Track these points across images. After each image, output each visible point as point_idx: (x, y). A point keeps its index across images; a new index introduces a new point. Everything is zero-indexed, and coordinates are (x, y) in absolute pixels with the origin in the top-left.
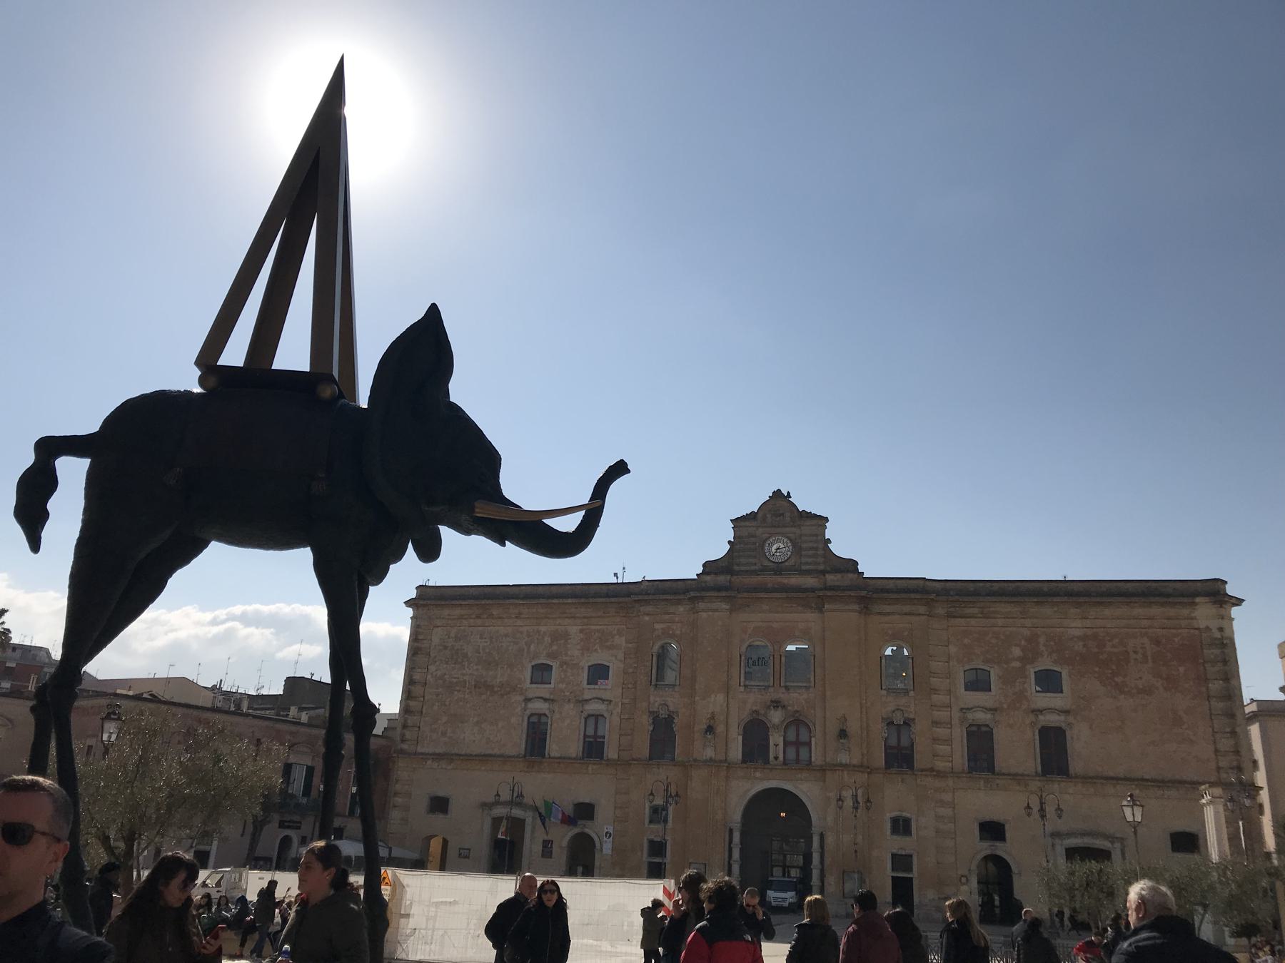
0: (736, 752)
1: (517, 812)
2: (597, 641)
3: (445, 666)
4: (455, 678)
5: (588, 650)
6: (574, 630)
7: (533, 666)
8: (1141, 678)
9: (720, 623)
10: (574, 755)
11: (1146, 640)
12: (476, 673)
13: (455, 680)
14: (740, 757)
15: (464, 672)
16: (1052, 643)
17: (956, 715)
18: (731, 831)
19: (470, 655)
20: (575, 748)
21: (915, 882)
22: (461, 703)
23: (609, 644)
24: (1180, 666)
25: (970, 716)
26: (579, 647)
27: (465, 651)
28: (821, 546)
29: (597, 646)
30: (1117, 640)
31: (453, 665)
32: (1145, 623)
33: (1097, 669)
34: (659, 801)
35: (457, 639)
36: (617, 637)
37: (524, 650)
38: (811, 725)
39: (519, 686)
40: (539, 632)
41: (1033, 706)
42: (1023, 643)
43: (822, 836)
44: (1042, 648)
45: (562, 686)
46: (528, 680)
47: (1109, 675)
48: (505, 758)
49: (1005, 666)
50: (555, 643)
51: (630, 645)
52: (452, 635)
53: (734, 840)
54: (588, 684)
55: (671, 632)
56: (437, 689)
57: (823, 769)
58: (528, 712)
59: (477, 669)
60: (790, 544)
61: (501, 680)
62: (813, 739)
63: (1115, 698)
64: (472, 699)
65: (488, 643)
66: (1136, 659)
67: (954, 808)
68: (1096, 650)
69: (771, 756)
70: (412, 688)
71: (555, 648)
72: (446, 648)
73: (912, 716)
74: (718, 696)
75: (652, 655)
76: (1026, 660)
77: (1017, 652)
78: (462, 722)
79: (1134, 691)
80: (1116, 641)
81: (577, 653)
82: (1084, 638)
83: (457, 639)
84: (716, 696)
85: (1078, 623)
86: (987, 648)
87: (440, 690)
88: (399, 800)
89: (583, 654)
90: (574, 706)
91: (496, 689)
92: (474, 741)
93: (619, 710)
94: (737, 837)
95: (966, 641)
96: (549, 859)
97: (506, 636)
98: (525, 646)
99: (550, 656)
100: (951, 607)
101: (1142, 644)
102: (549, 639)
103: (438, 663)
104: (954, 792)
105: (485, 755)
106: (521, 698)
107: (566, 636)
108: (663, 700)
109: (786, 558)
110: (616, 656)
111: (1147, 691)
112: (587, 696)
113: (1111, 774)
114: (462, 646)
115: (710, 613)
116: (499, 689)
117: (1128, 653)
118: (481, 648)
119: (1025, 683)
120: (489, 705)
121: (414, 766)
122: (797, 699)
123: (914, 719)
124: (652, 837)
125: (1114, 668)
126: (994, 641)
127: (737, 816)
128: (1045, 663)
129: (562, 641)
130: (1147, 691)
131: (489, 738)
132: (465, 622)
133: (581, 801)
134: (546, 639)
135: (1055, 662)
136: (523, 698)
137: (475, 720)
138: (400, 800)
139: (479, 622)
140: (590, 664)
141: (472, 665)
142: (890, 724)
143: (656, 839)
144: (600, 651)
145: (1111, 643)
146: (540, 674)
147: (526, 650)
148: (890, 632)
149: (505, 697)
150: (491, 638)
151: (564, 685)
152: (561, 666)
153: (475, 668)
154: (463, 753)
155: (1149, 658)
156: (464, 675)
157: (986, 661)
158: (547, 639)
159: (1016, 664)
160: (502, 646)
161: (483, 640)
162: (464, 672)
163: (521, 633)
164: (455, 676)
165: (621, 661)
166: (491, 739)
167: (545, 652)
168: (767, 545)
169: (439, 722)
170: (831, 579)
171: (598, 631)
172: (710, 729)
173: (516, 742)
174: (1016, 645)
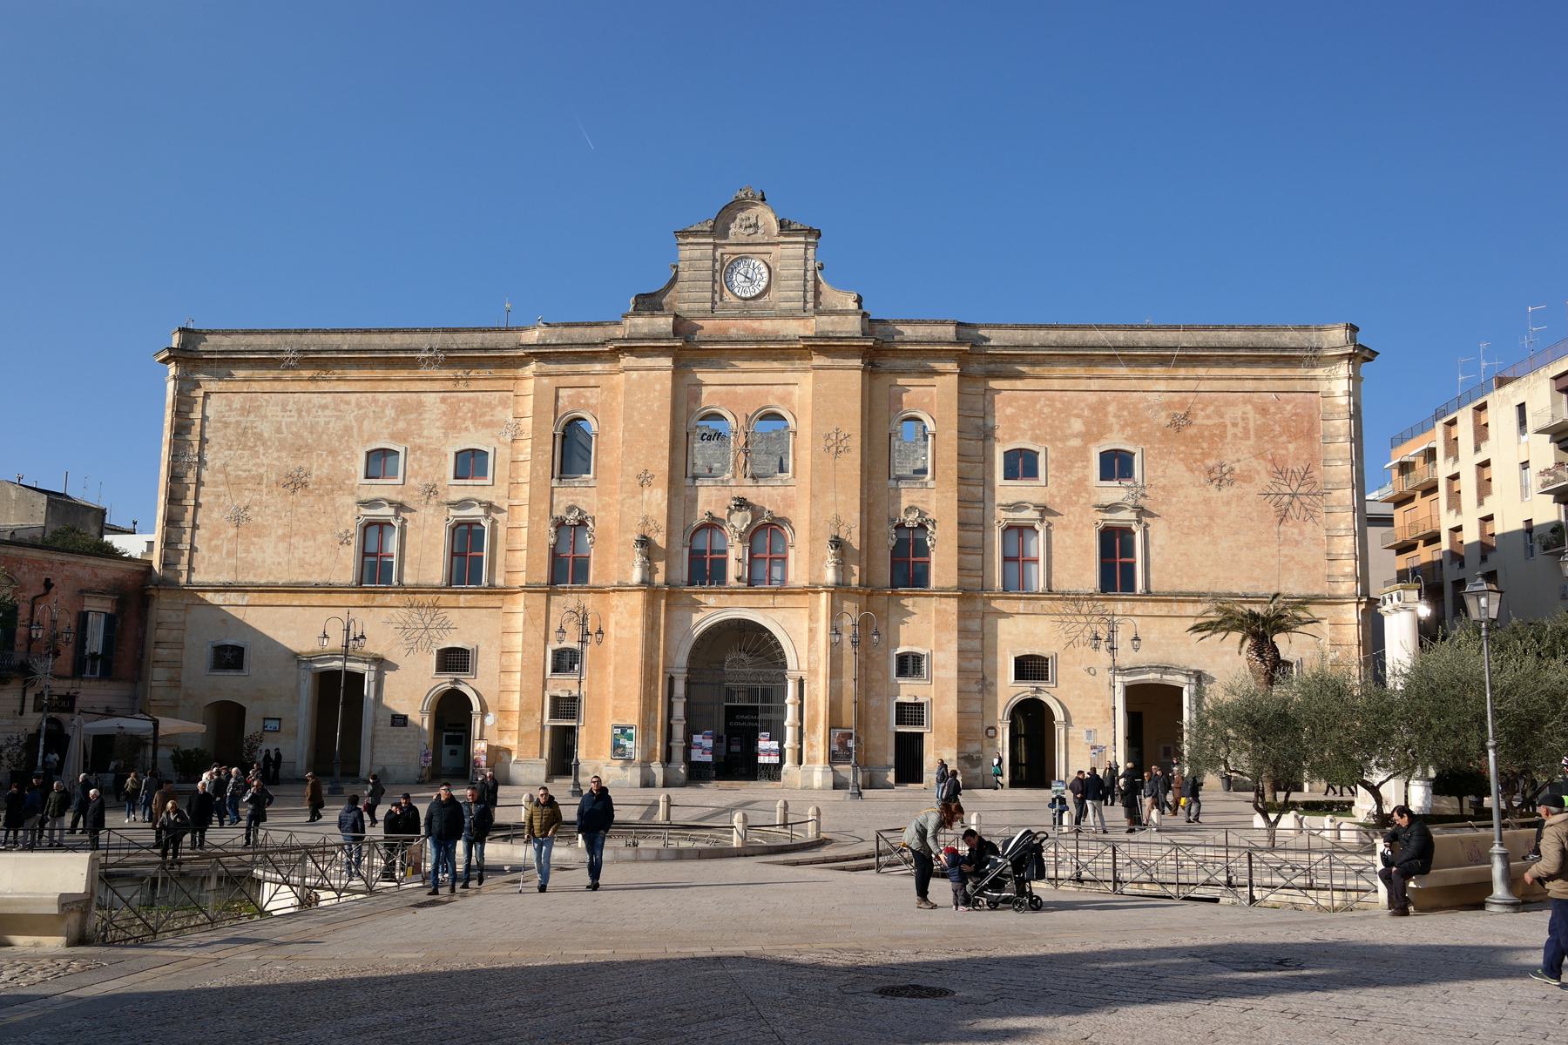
1: (354, 666)
2: (469, 415)
3: (227, 453)
4: (245, 471)
5: (455, 428)
6: (430, 399)
7: (368, 453)
9: (658, 387)
11: (1249, 407)
12: (275, 462)
13: (244, 475)
14: (686, 578)
15: (258, 461)
16: (1125, 413)
18: (671, 680)
19: (266, 435)
20: (436, 572)
22: (256, 509)
23: (487, 418)
24: (1290, 442)
26: (438, 424)
27: (258, 430)
29: (469, 423)
30: (1212, 408)
31: (239, 452)
32: (1249, 385)
33: (1182, 448)
34: (571, 643)
35: (245, 411)
36: (500, 408)
37: (352, 428)
39: (347, 482)
40: (375, 401)
41: (1095, 500)
42: (1086, 413)
43: (801, 682)
44: (1112, 420)
46: (362, 473)
47: (1199, 457)
48: (329, 589)
49: (1060, 446)
50: (402, 417)
52: (236, 405)
53: (676, 691)
54: (456, 478)
55: (582, 401)
56: (215, 487)
59: (279, 458)
61: (319, 473)
63: (1205, 486)
64: (273, 501)
65: (295, 419)
66: (1235, 435)
67: (983, 639)
70: (176, 487)
71: (401, 425)
72: (226, 425)
74: (655, 491)
75: (554, 435)
76: (1088, 437)
77: (1077, 425)
78: (259, 537)
80: (1210, 409)
81: (438, 433)
82: (1168, 405)
83: (245, 411)
84: (651, 492)
85: (1162, 385)
86: (1036, 420)
87: (222, 489)
88: (162, 653)
89: (446, 435)
90: (435, 510)
91: (311, 487)
92: (279, 563)
94: (680, 688)
97: (325, 407)
98: (354, 423)
99: (394, 437)
100: (990, 363)
101: (1244, 413)
103: (215, 449)
104: (983, 618)
105: (297, 585)
106: (351, 500)
107: (420, 404)
109: (757, 292)
112: (456, 496)
113: (1192, 588)
114: (253, 422)
116: (316, 487)
117: (1226, 426)
118: (283, 424)
119: (1085, 467)
120: (302, 510)
121: (185, 601)
122: (766, 496)
125: (1205, 445)
126: (1046, 410)
127: (682, 660)
128: (1115, 442)
129: (413, 416)
131: (303, 559)
132: (255, 386)
133: (449, 646)
134: (387, 412)
135: (1129, 439)
136: (355, 499)
137: (280, 532)
138: (166, 652)
139: (278, 386)
140: (458, 449)
141: (270, 451)
143: (561, 695)
144: (472, 429)
145: (1203, 413)
146: (379, 461)
147: (355, 430)
149: (326, 498)
150: (299, 411)
153: (276, 455)
154: (263, 581)
155: (1252, 433)
156: (258, 465)
157: (1035, 439)
158: (390, 413)
159: (1075, 443)
160: (317, 423)
161: (288, 413)
162: (258, 461)
163: (348, 403)
164: (244, 468)
165: (505, 444)
166: (307, 560)
167: (386, 431)
169: (223, 536)
171: (469, 400)
173: (345, 567)
174: (1078, 416)
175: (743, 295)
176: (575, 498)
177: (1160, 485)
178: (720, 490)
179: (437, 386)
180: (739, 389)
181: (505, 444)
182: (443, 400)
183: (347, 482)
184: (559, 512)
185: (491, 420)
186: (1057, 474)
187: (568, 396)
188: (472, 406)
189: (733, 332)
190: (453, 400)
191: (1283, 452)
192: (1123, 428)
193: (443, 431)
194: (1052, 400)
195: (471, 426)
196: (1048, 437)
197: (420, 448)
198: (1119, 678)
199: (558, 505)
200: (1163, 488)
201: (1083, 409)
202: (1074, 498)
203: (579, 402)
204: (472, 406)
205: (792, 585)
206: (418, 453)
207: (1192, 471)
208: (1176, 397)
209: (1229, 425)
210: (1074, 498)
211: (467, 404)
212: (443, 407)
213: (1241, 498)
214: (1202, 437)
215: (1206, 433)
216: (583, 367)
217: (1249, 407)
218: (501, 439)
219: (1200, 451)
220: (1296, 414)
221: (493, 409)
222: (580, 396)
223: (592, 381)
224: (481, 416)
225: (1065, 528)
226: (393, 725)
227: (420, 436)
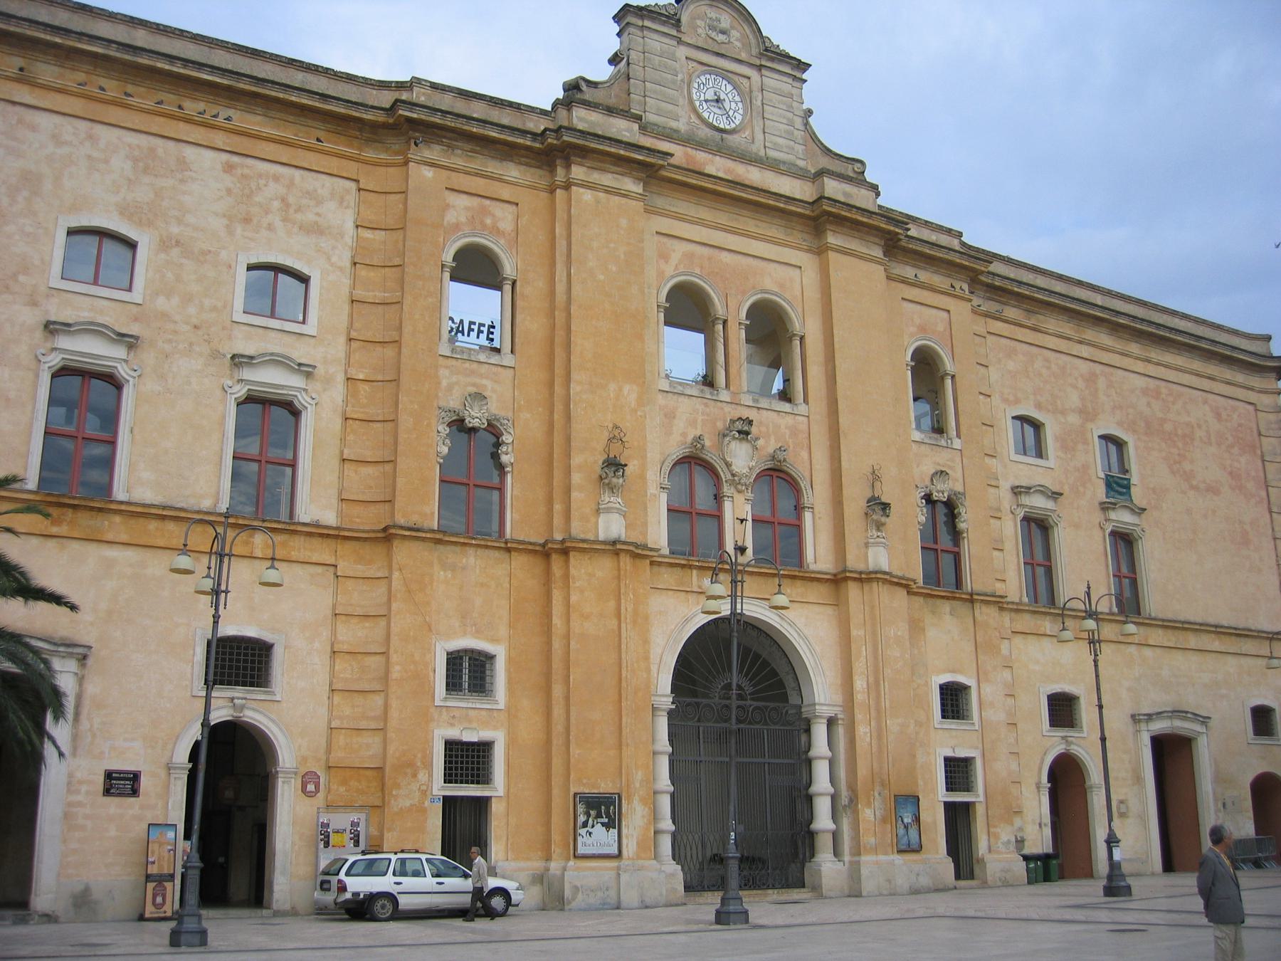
0: (658, 534)
5: (247, 220)
8: (1207, 468)
10: (206, 504)
11: (1207, 408)
17: (1006, 499)
21: (980, 811)
23: (310, 217)
25: (1026, 500)
28: (798, 122)
33: (1164, 445)
38: (804, 485)
42: (1081, 384)
45: (161, 303)
50: (146, 179)
51: (367, 234)
55: (488, 221)
57: (838, 580)
58: (55, 360)
60: (737, 98)
62: (808, 516)
68: (1160, 415)
69: (730, 547)
71: (142, 194)
73: (959, 488)
76: (1088, 414)
79: (1202, 486)
81: (218, 224)
82: (1145, 391)
89: (230, 230)
93: (336, 394)
95: (1011, 365)
96: (132, 799)
99: (125, 211)
102: (128, 165)
107: (183, 164)
108: (474, 385)
110: (329, 259)
111: (1213, 490)
115: (601, 195)
123: (964, 494)
124: (454, 733)
125: (1180, 445)
130: (1213, 490)
142: (928, 499)
148: (917, 321)
151: (175, 300)
152: (166, 244)
165: (341, 269)
168: (696, 85)
170: (833, 188)
172: (614, 465)
174: (1075, 387)
175: (715, 123)
176: (478, 381)
177: (1152, 486)
178: (706, 405)
179: (220, 139)
180: (726, 257)
181: (341, 269)
182: (229, 168)
183: (21, 278)
184: (454, 402)
185: (316, 223)
186: (1062, 455)
187: (467, 209)
188: (282, 191)
189: (710, 170)
190: (246, 171)
191: (1236, 464)
192: (1114, 408)
193: (225, 221)
194: (1047, 360)
195: (278, 224)
196: (1050, 407)
197: (178, 243)
198: (1085, 735)
199: (450, 388)
200: (1154, 490)
201: (1076, 379)
202: (1081, 489)
203: (482, 223)
204: (282, 191)
205: (812, 567)
206: (175, 252)
207: (1173, 473)
208: (1152, 384)
209: (1195, 426)
210: (1081, 489)
211: (272, 184)
212: (228, 181)
213: (1214, 512)
214: (1176, 435)
215: (1180, 432)
216: (494, 167)
217: (1207, 408)
218: (334, 259)
219: (1175, 451)
220: (1240, 425)
221: (319, 202)
222: (484, 211)
223: (506, 193)
224: (296, 211)
225: (1077, 526)
226: (107, 792)
227: (180, 221)
